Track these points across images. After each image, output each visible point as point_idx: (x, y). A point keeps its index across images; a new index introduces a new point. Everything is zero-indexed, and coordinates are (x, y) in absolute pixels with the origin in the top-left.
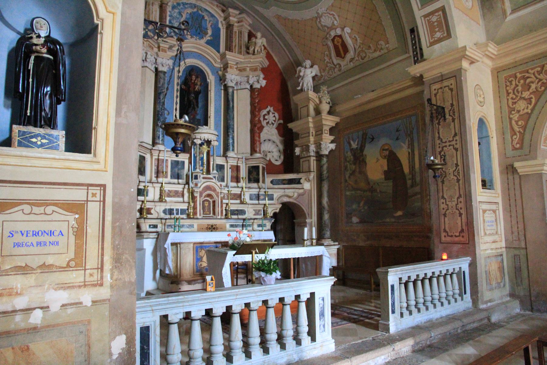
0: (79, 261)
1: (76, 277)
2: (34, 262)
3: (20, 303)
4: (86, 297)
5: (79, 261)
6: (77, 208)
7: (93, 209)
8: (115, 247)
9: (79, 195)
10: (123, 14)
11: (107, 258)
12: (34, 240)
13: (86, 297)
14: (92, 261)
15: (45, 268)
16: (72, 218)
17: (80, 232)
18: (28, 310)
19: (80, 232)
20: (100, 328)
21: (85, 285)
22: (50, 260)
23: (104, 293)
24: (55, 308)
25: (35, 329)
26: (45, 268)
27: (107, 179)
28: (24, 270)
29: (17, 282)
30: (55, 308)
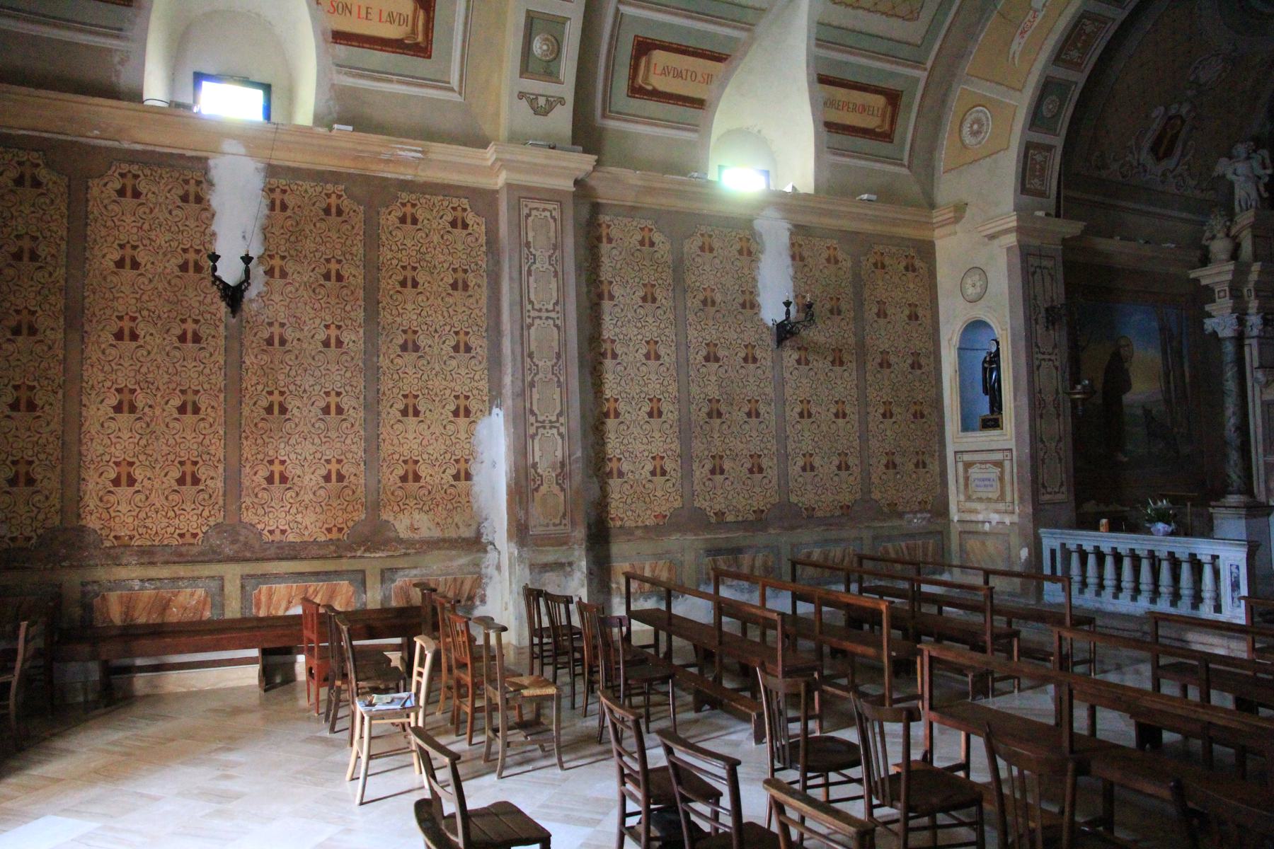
0: (1002, 498)
1: (1001, 506)
2: (984, 496)
3: (980, 517)
4: (1007, 520)
5: (1002, 498)
6: (999, 464)
7: (1007, 464)
8: (1019, 490)
9: (998, 456)
10: (1012, 328)
11: (1016, 496)
12: (982, 483)
13: (1007, 520)
14: (1008, 498)
15: (989, 500)
16: (998, 470)
17: (1001, 479)
18: (983, 522)
19: (1001, 479)
20: (1015, 540)
21: (1006, 512)
22: (990, 496)
23: (1015, 518)
24: (994, 523)
25: (986, 533)
26: (989, 500)
27: (1012, 444)
28: (980, 500)
29: (978, 506)
30: (994, 523)
